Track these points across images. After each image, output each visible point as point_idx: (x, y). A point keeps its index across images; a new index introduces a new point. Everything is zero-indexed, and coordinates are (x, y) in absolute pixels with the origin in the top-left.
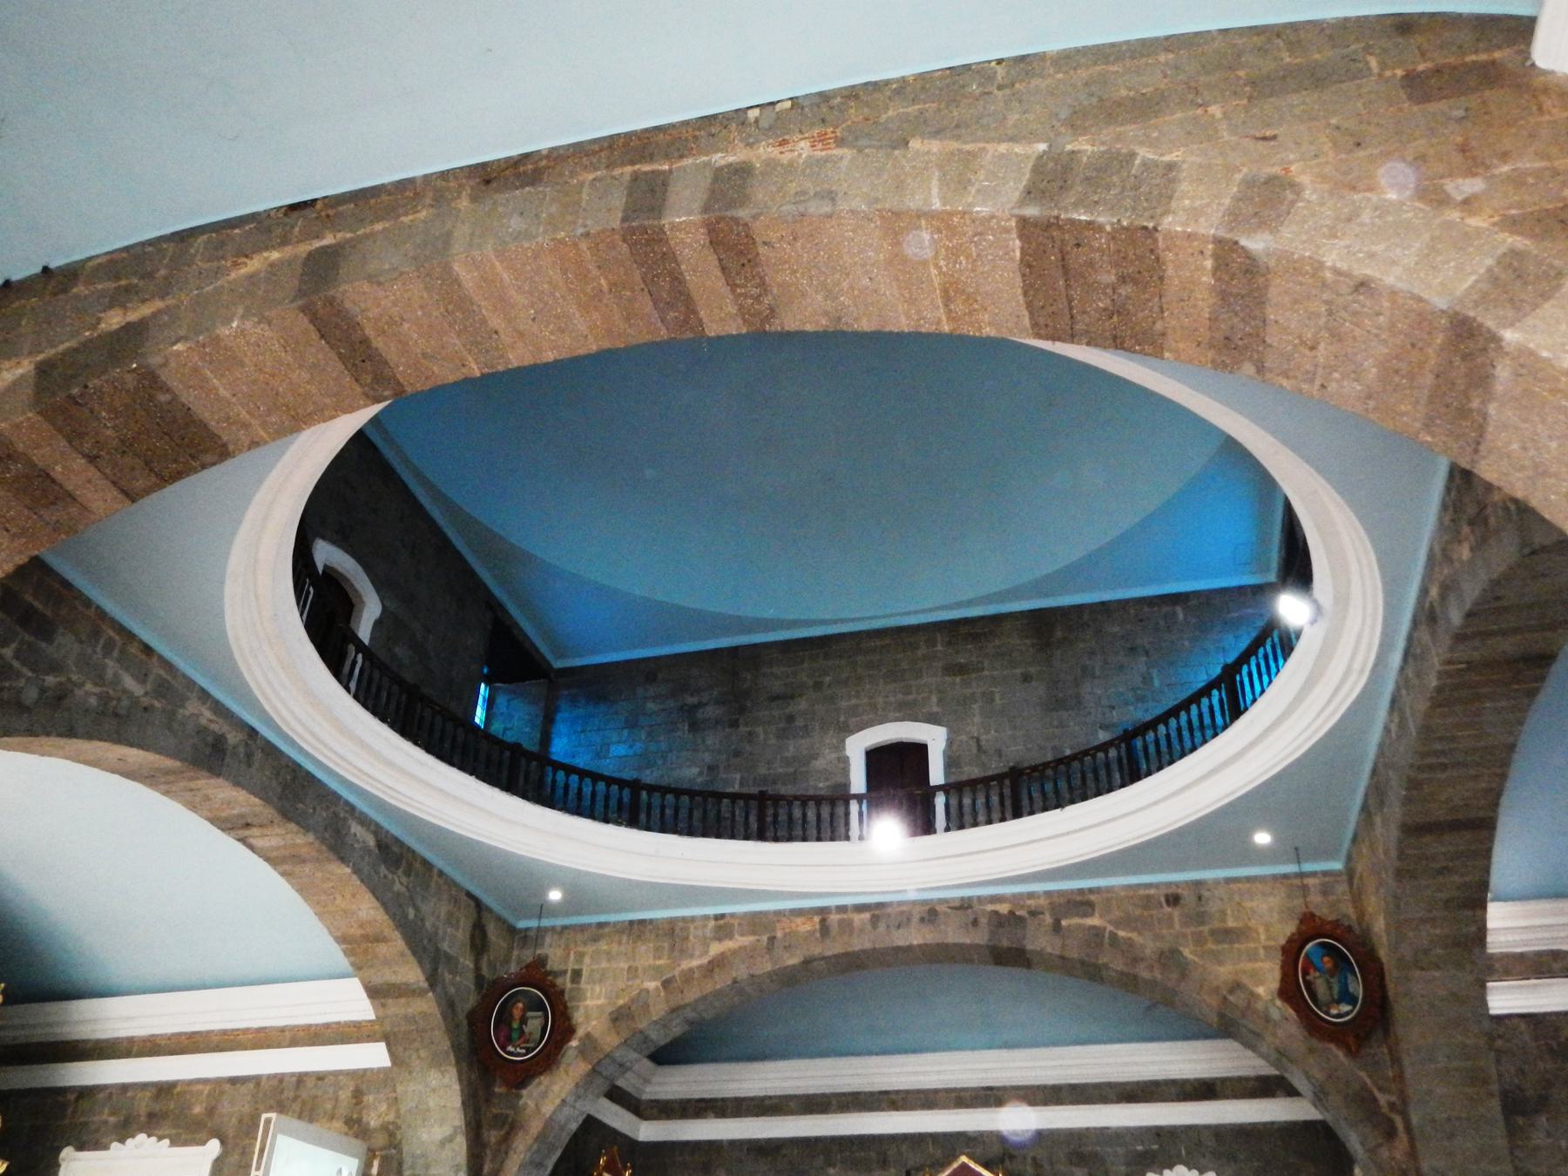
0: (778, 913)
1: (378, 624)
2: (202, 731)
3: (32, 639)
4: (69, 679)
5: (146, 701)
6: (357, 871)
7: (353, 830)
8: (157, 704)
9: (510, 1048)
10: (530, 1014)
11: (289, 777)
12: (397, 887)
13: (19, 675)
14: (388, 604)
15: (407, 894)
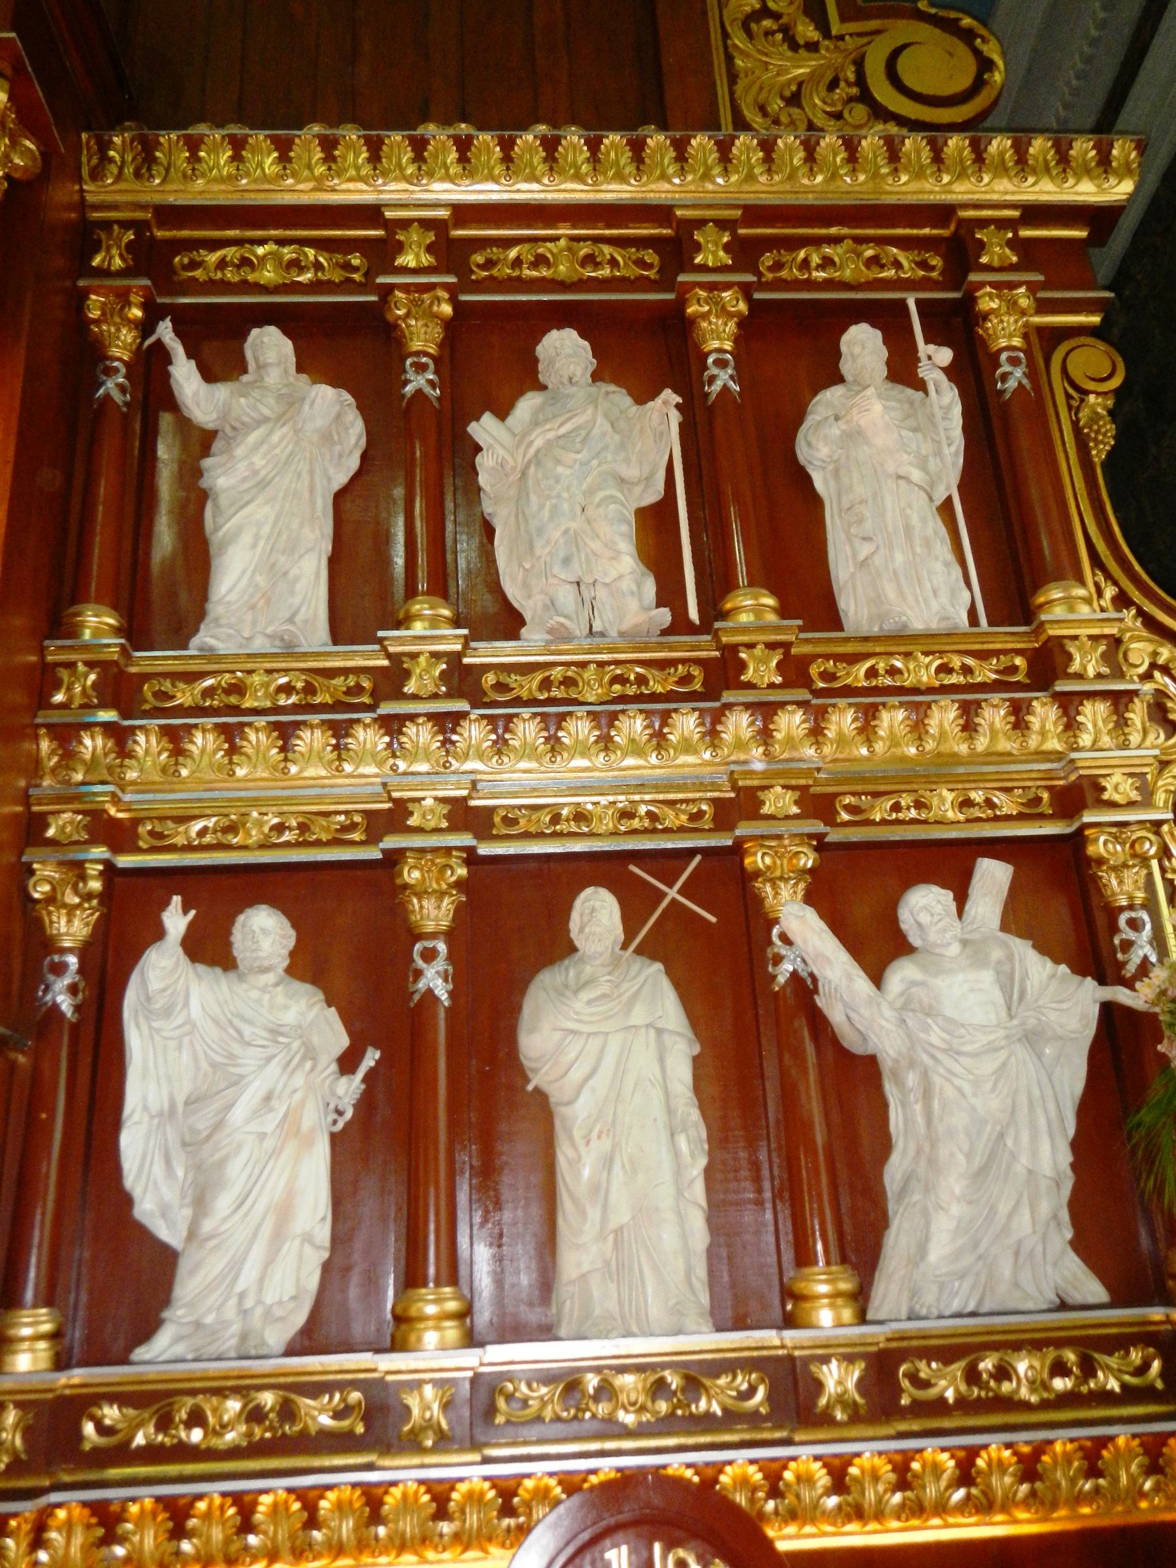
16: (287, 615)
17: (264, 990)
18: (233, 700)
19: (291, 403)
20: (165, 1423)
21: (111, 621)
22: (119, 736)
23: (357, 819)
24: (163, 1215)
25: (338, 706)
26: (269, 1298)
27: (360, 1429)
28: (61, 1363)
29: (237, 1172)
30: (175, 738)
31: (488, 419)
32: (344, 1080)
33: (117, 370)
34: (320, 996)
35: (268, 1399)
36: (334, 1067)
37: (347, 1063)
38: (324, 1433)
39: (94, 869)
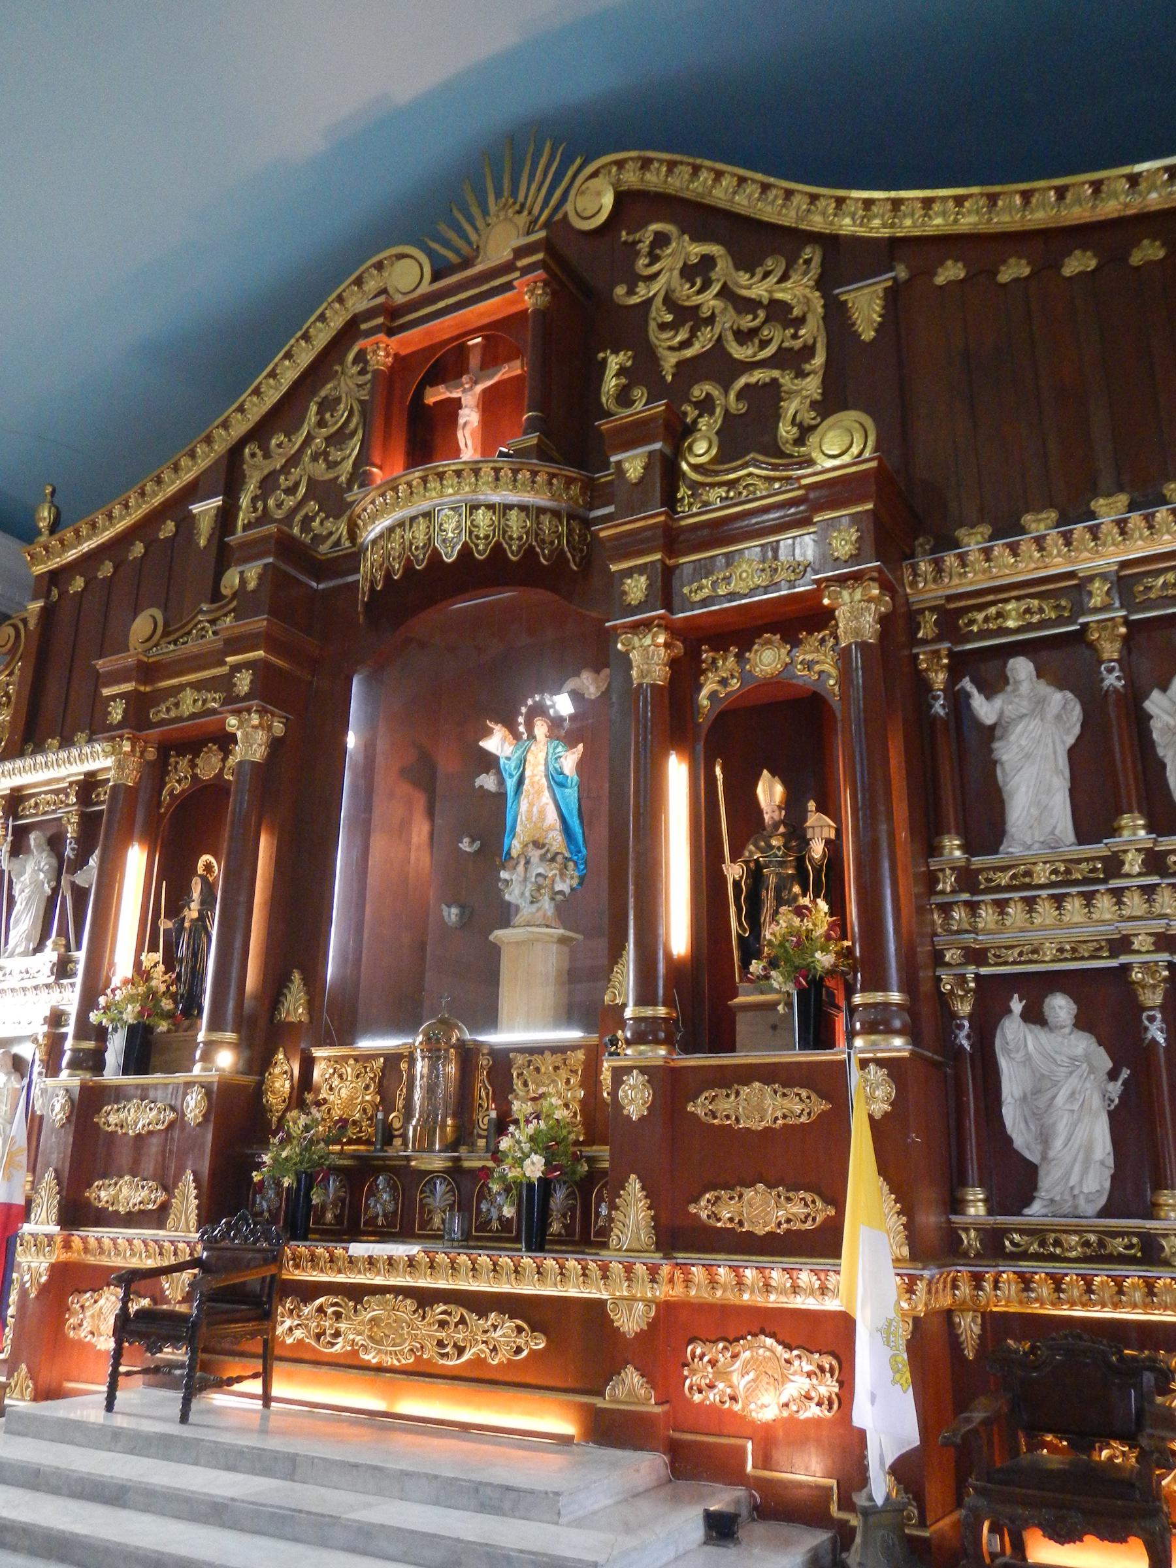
16: (1049, 829)
17: (1064, 1037)
18: (1027, 880)
19: (1040, 703)
20: (1042, 1244)
21: (957, 842)
22: (973, 907)
23: (1103, 943)
24: (1028, 1148)
25: (1085, 881)
26: (1086, 1190)
27: (1139, 1254)
28: (990, 1212)
29: (1062, 1128)
30: (1001, 905)
31: (1156, 695)
32: (1112, 1084)
33: (939, 697)
34: (1094, 1040)
35: (1093, 1238)
36: (1106, 1077)
37: (1113, 1075)
38: (1120, 1255)
39: (970, 976)
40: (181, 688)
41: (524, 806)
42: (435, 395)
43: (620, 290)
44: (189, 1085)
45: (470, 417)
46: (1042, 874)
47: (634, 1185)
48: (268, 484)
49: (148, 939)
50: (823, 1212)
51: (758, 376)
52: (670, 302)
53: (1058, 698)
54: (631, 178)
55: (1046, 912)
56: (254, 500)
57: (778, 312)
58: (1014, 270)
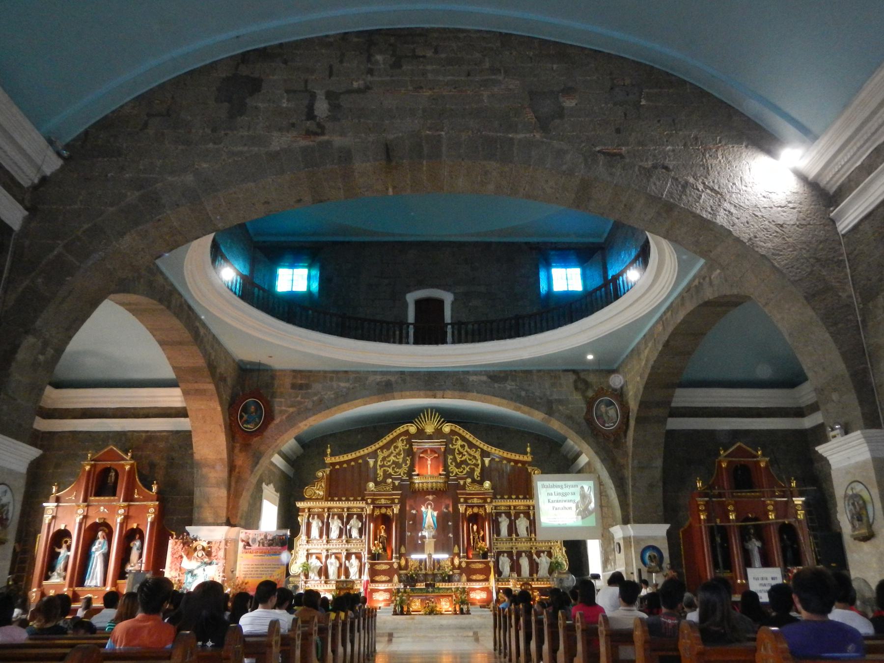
0: (654, 326)
1: (453, 303)
2: (378, 384)
3: (305, 391)
4: (322, 395)
5: (351, 386)
6: (478, 392)
7: (471, 379)
8: (357, 385)
9: (607, 425)
10: (608, 408)
11: (427, 378)
12: (509, 387)
13: (305, 402)
14: (457, 291)
15: (517, 388)
40: (381, 499)
41: (427, 520)
42: (421, 455)
43: (450, 445)
44: (394, 563)
45: (429, 462)
46: (504, 540)
47: (464, 574)
48: (384, 459)
49: (375, 539)
50: (485, 577)
51: (472, 467)
52: (458, 450)
53: (508, 520)
54: (453, 428)
55: (505, 544)
56: (381, 461)
57: (475, 457)
58: (505, 462)
